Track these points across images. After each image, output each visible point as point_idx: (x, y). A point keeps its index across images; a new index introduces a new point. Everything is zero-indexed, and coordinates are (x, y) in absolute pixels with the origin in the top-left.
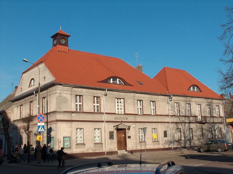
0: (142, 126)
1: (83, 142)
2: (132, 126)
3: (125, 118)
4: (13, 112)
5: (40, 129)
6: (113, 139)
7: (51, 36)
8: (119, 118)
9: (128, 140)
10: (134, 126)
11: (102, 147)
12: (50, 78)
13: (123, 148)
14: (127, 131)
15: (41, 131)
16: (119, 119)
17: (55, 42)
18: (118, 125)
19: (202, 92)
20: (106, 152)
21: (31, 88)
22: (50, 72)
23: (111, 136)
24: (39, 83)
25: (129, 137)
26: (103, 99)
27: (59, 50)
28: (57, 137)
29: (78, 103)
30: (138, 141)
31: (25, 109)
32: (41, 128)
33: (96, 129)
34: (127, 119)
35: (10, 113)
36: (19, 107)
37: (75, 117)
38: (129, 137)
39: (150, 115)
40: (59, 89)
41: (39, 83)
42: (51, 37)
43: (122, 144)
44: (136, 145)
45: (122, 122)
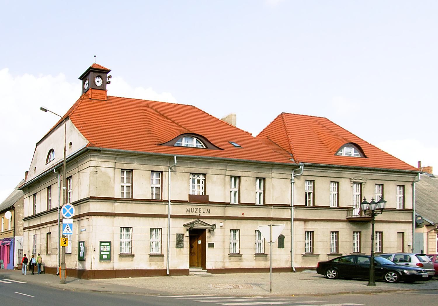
0: (234, 225)
1: (131, 252)
2: (218, 223)
3: (206, 210)
4: (23, 206)
5: (66, 229)
6: (183, 247)
7: (79, 77)
8: (195, 210)
9: (208, 250)
10: (221, 224)
11: (163, 260)
12: (80, 142)
13: (196, 264)
14: (208, 234)
15: (68, 232)
16: (195, 211)
17: (86, 86)
18: (192, 223)
19: (366, 157)
20: (170, 270)
21: (50, 165)
22: (79, 132)
23: (179, 243)
24: (65, 147)
25: (211, 245)
26: (167, 175)
27: (93, 98)
28: (90, 241)
29: (125, 184)
30: (227, 253)
31: (39, 200)
32: (68, 227)
33: (153, 229)
34: (209, 211)
35: (20, 208)
36: (32, 197)
37: (119, 208)
38: (211, 245)
39: (254, 205)
40: (93, 161)
41: (65, 147)
42: (79, 79)
43: (198, 257)
44: (224, 259)
45: (200, 217)
